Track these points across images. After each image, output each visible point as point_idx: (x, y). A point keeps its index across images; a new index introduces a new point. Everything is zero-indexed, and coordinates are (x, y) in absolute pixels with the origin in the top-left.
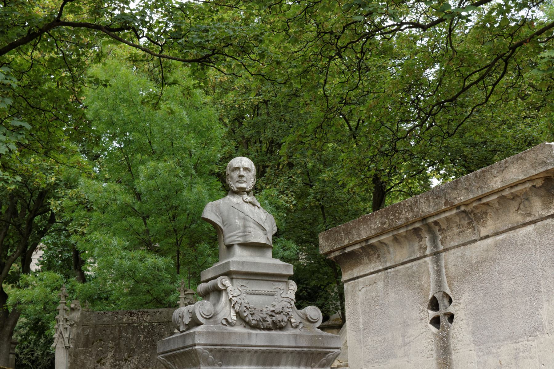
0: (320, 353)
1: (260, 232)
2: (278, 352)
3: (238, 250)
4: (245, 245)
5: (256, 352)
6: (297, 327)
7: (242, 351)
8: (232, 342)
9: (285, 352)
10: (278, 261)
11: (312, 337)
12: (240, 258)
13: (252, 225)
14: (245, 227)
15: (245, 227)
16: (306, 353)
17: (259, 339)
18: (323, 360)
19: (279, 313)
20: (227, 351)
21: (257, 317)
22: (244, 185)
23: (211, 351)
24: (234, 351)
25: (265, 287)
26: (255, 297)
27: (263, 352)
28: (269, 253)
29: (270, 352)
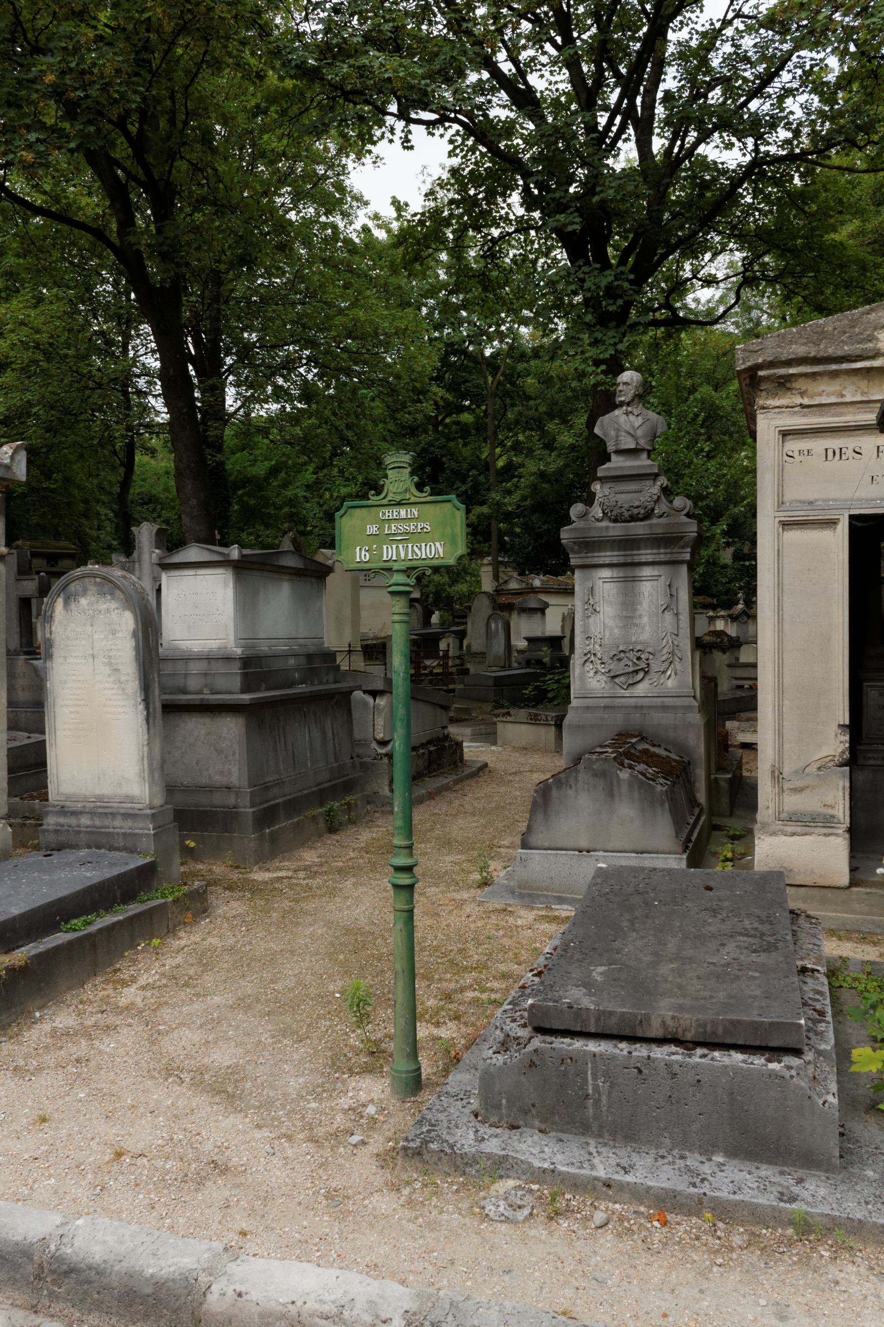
0: (675, 538)
1: (630, 439)
2: (635, 540)
3: (614, 457)
4: (619, 452)
5: (614, 541)
6: (661, 517)
7: (602, 541)
8: (591, 535)
9: (641, 539)
10: (649, 462)
11: (667, 525)
12: (617, 463)
13: (623, 434)
14: (617, 436)
15: (617, 436)
16: (661, 538)
17: (617, 530)
18: (681, 543)
19: (637, 507)
20: (588, 542)
21: (614, 513)
22: (623, 399)
23: (575, 543)
24: (594, 542)
25: (633, 486)
26: (623, 496)
27: (621, 541)
28: (644, 455)
29: (627, 540)
